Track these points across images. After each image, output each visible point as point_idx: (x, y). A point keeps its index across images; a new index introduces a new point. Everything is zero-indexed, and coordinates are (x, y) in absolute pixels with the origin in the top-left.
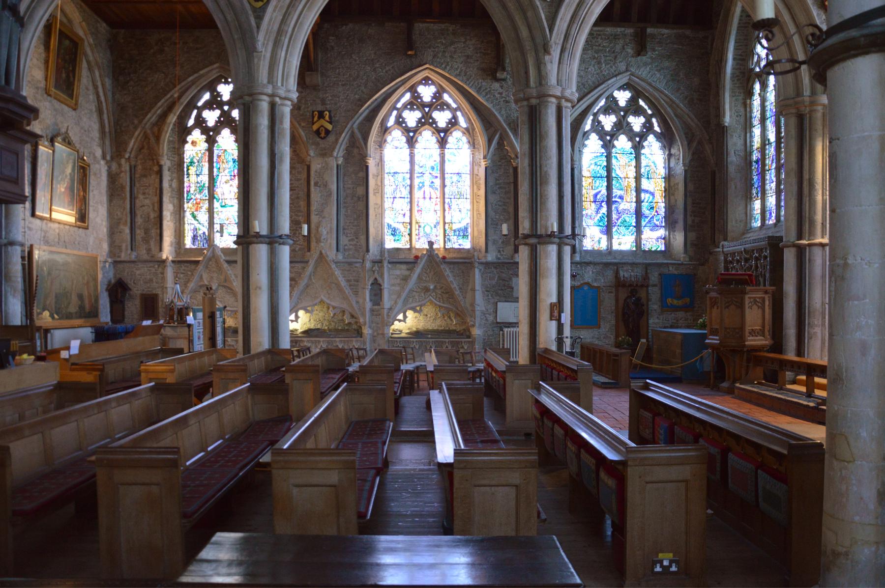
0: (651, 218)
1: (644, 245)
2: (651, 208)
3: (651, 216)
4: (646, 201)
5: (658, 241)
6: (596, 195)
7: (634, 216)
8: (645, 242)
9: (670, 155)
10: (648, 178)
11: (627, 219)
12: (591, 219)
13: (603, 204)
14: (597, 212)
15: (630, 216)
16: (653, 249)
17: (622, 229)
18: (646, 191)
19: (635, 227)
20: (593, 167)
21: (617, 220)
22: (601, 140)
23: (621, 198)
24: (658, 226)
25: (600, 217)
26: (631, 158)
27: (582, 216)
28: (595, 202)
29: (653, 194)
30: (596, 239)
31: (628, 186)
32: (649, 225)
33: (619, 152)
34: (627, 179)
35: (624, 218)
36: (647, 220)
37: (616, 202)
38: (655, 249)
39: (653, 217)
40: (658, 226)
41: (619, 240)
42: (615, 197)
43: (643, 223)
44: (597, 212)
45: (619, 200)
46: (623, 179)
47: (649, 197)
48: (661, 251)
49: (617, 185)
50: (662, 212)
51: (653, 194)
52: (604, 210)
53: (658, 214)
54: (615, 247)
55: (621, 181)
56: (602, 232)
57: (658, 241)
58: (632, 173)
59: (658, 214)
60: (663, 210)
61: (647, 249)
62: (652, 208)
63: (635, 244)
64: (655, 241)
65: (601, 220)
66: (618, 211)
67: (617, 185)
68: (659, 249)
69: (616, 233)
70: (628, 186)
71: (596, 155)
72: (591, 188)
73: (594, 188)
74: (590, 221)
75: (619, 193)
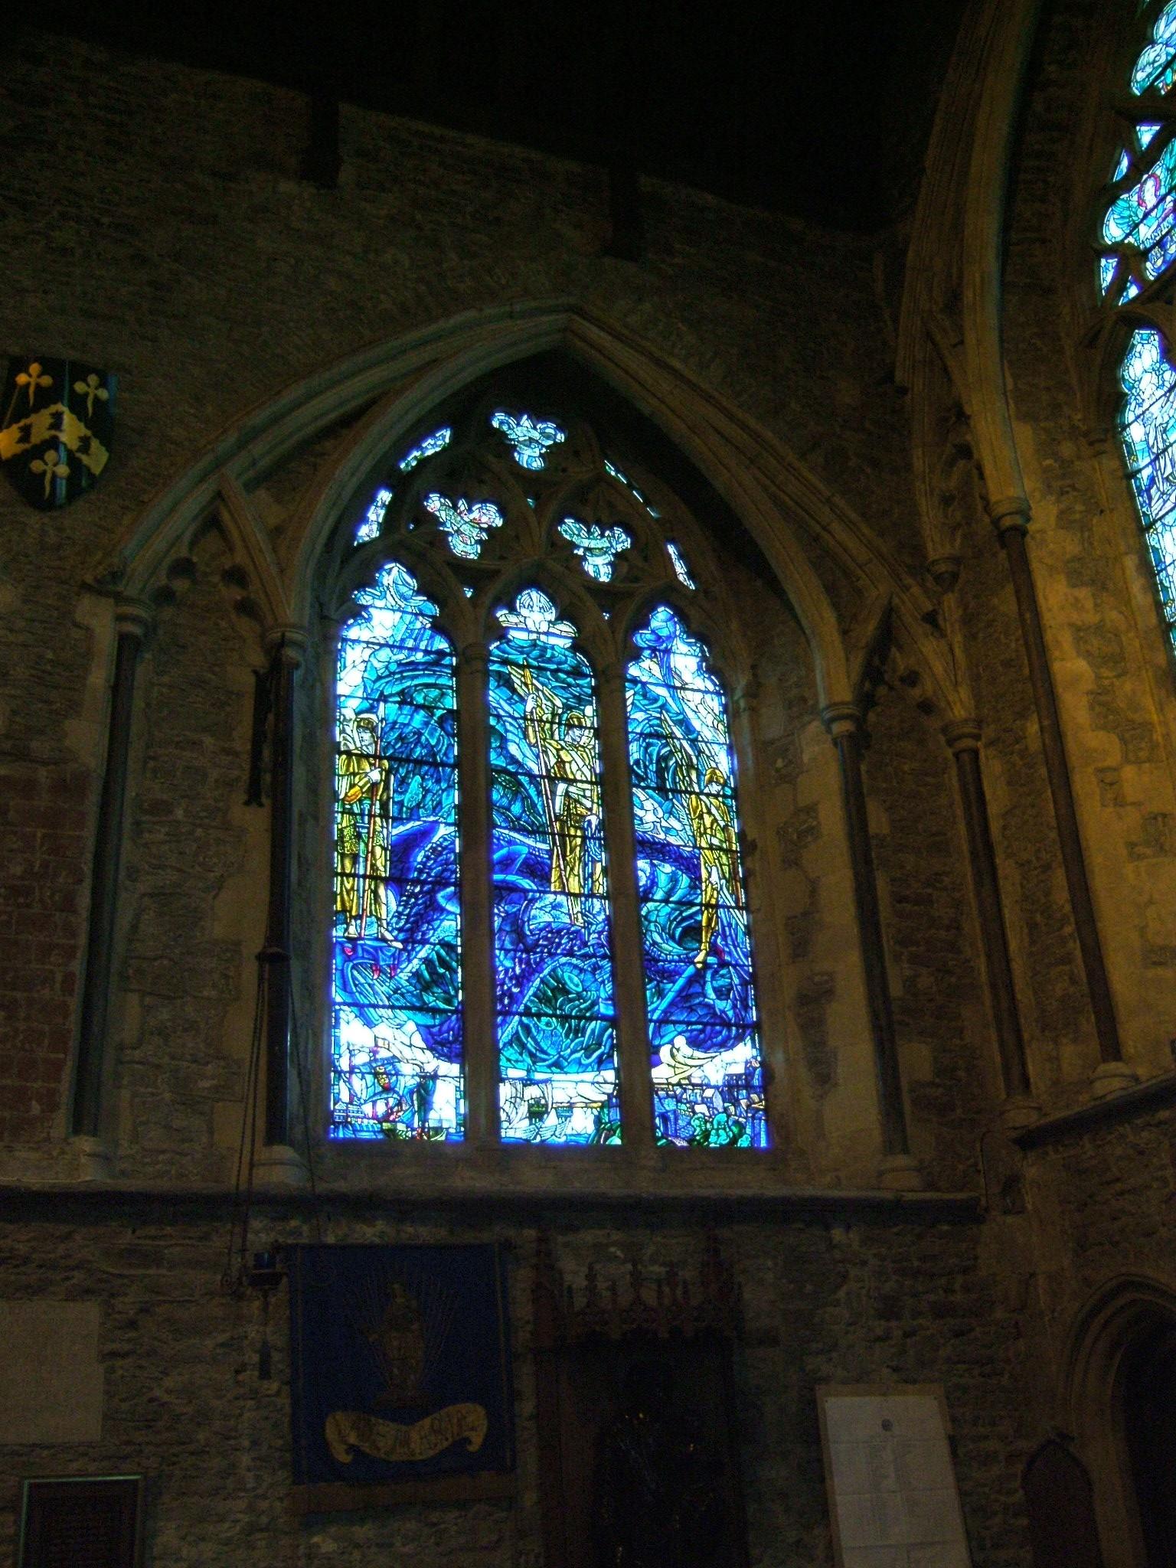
0: (691, 981)
1: (664, 1117)
2: (686, 932)
3: (690, 970)
4: (659, 895)
5: (736, 1103)
6: (401, 850)
7: (606, 964)
8: (670, 1105)
9: (754, 692)
10: (661, 790)
11: (573, 981)
12: (377, 968)
13: (440, 897)
14: (412, 936)
15: (586, 965)
16: (714, 1142)
17: (546, 1026)
18: (659, 850)
19: (613, 1021)
20: (387, 710)
21: (522, 980)
22: (432, 598)
23: (537, 870)
24: (727, 1025)
25: (427, 961)
26: (576, 691)
27: (330, 948)
28: (397, 881)
29: (689, 865)
30: (407, 1081)
31: (571, 817)
32: (683, 1017)
33: (520, 659)
34: (561, 787)
35: (553, 974)
36: (672, 989)
37: (513, 888)
38: (724, 1139)
39: (698, 978)
40: (727, 1025)
41: (533, 1092)
42: (507, 863)
43: (657, 1007)
44: (412, 936)
45: (526, 883)
46: (545, 784)
47: (674, 880)
48: (753, 1150)
49: (516, 808)
50: (740, 952)
51: (689, 865)
52: (448, 927)
53: (723, 964)
54: (516, 1127)
55: (532, 792)
56: (435, 1043)
57: (736, 1103)
58: (582, 765)
59: (723, 964)
60: (747, 943)
61: (680, 1143)
62: (692, 932)
63: (615, 1114)
64: (718, 1102)
65: (430, 979)
66: (519, 934)
67: (516, 808)
68: (744, 1142)
69: (510, 1053)
70: (571, 817)
71: (401, 656)
72: (377, 809)
73: (392, 810)
74: (373, 977)
75: (527, 845)
